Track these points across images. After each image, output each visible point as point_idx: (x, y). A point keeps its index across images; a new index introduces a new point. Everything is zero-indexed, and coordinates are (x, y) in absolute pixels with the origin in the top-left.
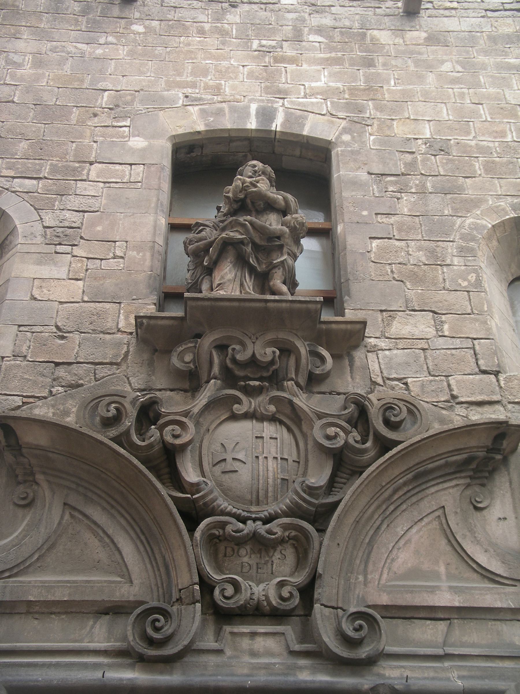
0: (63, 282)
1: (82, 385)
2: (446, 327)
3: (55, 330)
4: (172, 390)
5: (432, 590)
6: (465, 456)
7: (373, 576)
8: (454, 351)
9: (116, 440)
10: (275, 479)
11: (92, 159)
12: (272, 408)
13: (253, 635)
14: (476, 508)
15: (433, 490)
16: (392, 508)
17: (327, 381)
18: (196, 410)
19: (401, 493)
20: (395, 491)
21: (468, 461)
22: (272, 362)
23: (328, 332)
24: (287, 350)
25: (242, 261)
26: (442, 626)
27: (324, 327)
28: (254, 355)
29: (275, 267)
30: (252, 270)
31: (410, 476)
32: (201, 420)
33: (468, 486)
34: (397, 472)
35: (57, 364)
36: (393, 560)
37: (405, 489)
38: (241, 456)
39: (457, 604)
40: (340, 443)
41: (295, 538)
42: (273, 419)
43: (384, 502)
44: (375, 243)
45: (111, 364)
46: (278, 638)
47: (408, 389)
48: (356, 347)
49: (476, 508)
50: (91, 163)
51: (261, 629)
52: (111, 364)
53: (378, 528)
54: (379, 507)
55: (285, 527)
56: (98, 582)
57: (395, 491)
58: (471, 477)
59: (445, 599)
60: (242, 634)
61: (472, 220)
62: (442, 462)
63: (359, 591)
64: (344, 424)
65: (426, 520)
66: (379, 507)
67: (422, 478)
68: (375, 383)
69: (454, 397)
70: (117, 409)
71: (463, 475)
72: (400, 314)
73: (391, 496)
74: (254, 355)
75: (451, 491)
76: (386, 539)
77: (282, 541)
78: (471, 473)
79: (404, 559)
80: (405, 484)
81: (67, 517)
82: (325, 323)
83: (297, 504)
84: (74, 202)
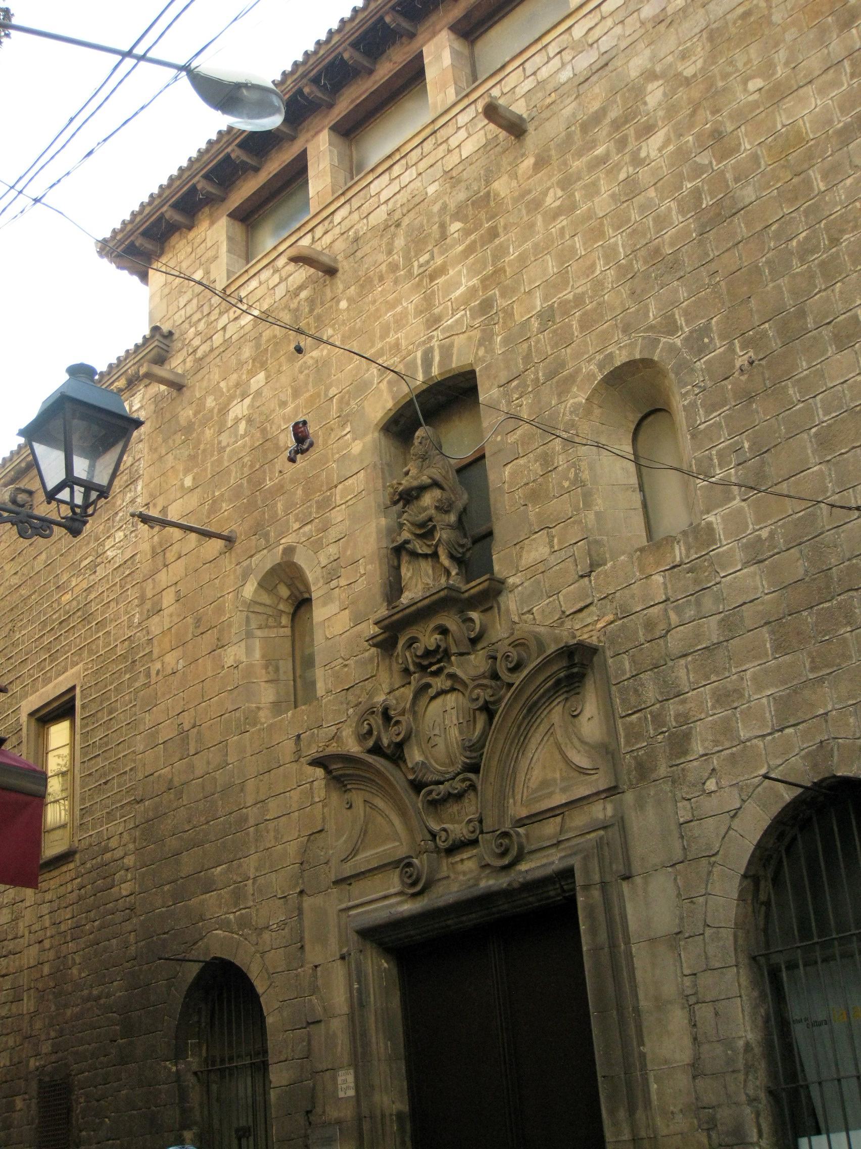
0: (338, 616)
1: (360, 703)
2: (556, 540)
3: (340, 661)
4: (403, 686)
5: (550, 795)
6: (553, 680)
7: (518, 797)
8: (560, 565)
9: (370, 751)
10: (457, 743)
11: (335, 483)
12: (449, 683)
13: (462, 860)
14: (574, 716)
15: (545, 713)
16: (522, 739)
17: (485, 636)
18: (408, 706)
19: (524, 725)
20: (519, 727)
21: (558, 683)
22: (438, 647)
23: (472, 597)
24: (444, 631)
25: (414, 555)
26: (559, 819)
27: (466, 595)
28: (426, 647)
29: (437, 546)
30: (425, 556)
31: (525, 711)
32: (416, 709)
33: (567, 699)
34: (516, 712)
35: (347, 689)
36: (529, 779)
37: (526, 721)
38: (437, 732)
39: (564, 802)
40: (481, 702)
41: (471, 785)
42: (453, 689)
43: (514, 738)
44: (508, 470)
45: (372, 677)
46: (474, 859)
47: (534, 619)
48: (499, 592)
49: (574, 716)
50: (336, 486)
51: (465, 856)
52: (372, 677)
53: (517, 757)
54: (512, 742)
55: (464, 780)
56: (389, 849)
57: (519, 727)
58: (567, 692)
59: (559, 799)
60: (456, 862)
61: (571, 401)
62: (542, 690)
63: (511, 812)
64: (485, 682)
65: (545, 739)
66: (512, 742)
67: (532, 710)
68: (515, 623)
69: (563, 612)
70: (368, 724)
71: (560, 693)
72: (526, 542)
73: (517, 733)
74: (426, 647)
75: (557, 708)
76: (524, 764)
77: (465, 791)
78: (565, 689)
79: (537, 775)
80: (524, 718)
81: (368, 809)
82: (466, 591)
83: (465, 763)
84: (333, 534)
